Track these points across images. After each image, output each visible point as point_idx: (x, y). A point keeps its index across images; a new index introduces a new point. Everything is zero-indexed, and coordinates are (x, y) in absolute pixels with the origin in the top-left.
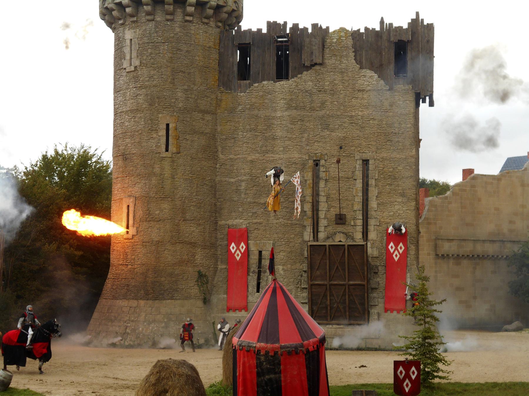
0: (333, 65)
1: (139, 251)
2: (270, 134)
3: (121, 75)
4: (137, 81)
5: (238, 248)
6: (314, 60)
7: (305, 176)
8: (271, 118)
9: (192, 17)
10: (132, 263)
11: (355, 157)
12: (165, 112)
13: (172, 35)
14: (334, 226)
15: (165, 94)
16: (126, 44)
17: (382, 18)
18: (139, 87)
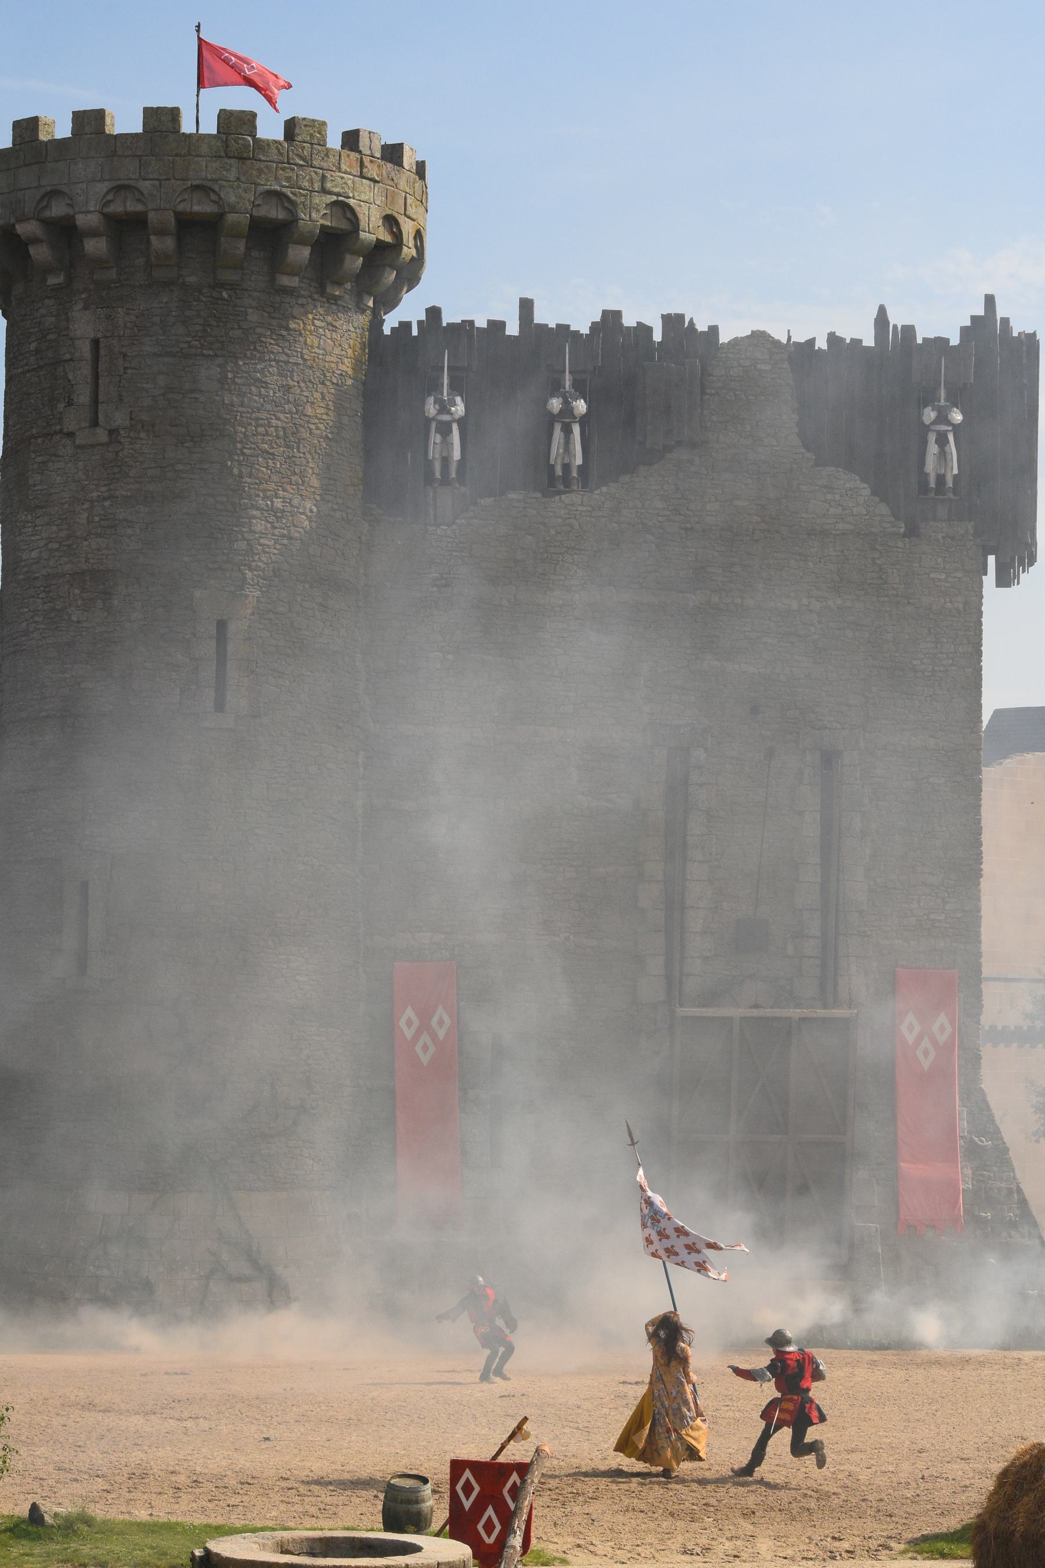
3: (55, 455)
4: (117, 476)
5: (424, 1027)
9: (297, 279)
12: (212, 582)
17: (882, 310)
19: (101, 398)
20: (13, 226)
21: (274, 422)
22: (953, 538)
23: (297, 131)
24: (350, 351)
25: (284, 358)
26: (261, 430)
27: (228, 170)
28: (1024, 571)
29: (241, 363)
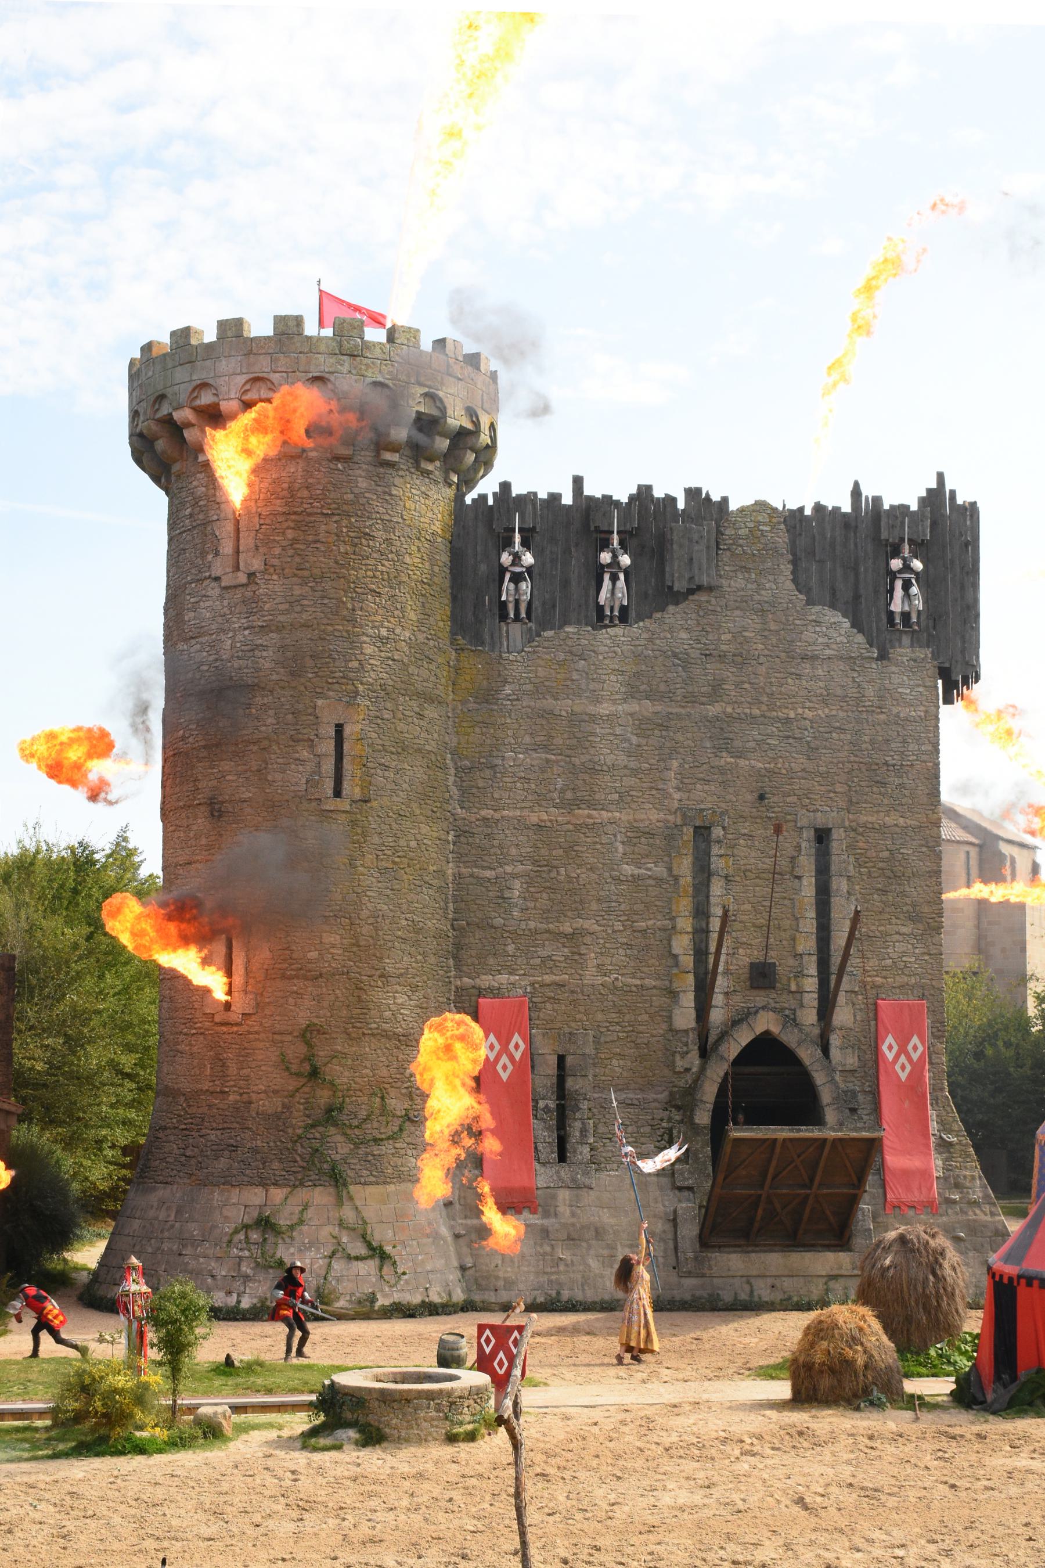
0: (742, 593)
1: (260, 1057)
2: (584, 758)
3: (205, 596)
6: (696, 578)
7: (675, 866)
8: (587, 718)
10: (240, 1088)
11: (795, 822)
12: (331, 693)
13: (351, 497)
14: (747, 992)
15: (331, 647)
16: (222, 515)
17: (856, 485)
18: (263, 626)
19: (241, 548)
20: (170, 414)
21: (380, 568)
22: (915, 661)
23: (396, 335)
24: (439, 516)
25: (387, 517)
26: (369, 573)
27: (341, 365)
28: (968, 688)
29: (353, 520)
